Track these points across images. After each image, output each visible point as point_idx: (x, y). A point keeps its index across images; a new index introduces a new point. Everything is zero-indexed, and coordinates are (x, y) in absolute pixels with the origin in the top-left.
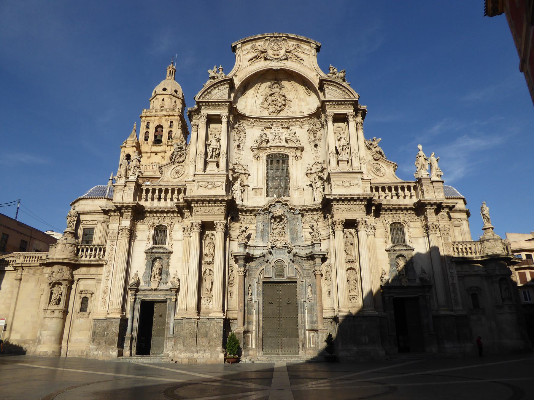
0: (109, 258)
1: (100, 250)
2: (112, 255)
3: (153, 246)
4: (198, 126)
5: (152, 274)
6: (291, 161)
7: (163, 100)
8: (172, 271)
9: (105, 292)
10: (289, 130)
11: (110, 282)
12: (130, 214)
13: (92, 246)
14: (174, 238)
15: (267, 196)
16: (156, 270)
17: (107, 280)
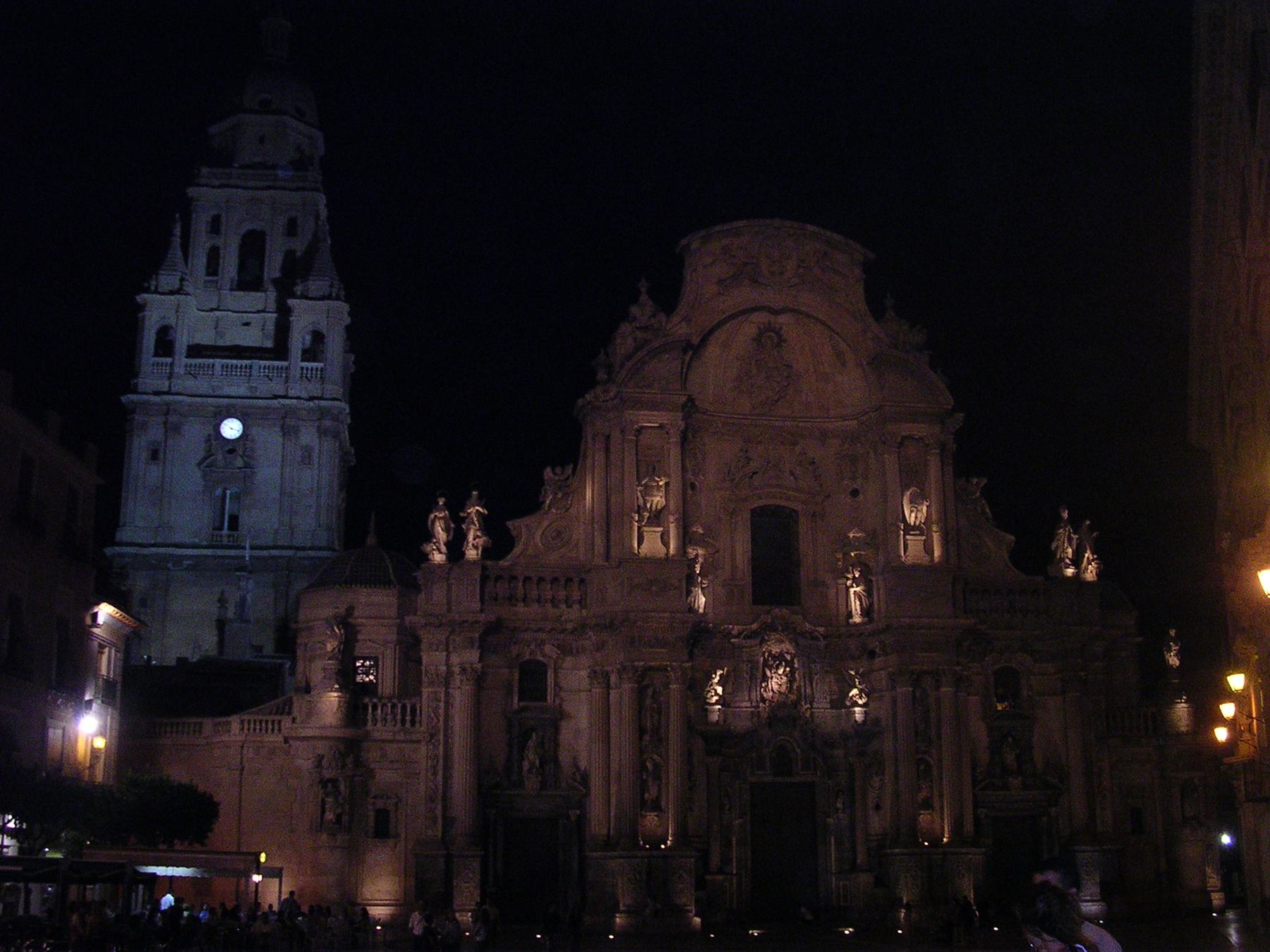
0: (433, 727)
1: (404, 707)
2: (439, 720)
3: (521, 704)
4: (608, 437)
5: (526, 765)
6: (804, 526)
7: (262, 140)
8: (564, 757)
9: (431, 799)
10: (798, 449)
11: (440, 777)
12: (477, 635)
13: (384, 701)
14: (563, 684)
15: (756, 601)
16: (531, 755)
17: (435, 774)
